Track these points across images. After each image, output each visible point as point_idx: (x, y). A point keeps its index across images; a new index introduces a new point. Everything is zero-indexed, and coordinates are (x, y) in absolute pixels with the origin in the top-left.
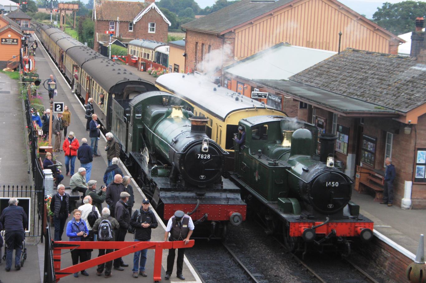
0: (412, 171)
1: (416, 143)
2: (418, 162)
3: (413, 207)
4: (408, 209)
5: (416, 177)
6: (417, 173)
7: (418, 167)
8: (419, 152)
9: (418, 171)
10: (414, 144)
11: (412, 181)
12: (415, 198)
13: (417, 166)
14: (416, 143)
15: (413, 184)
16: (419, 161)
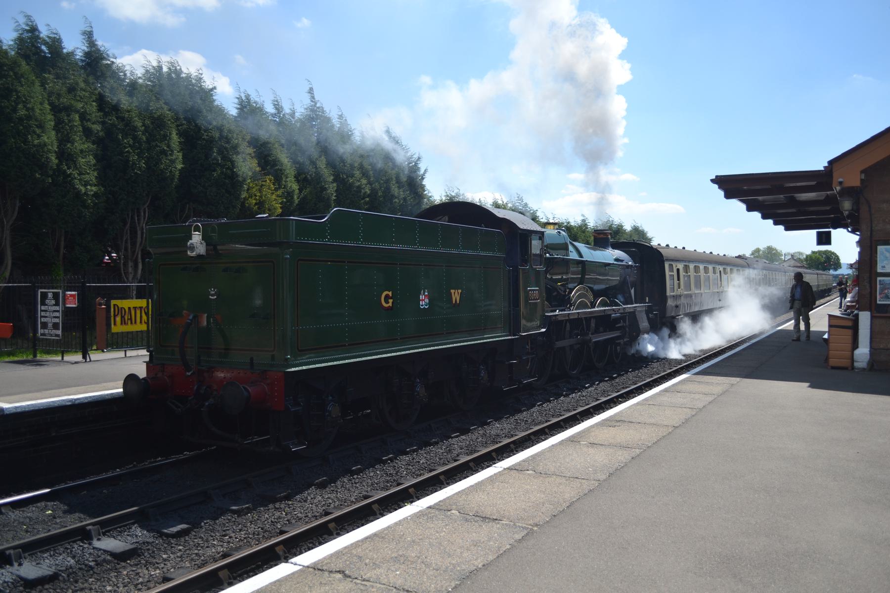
0: (869, 290)
1: (872, 231)
2: (879, 270)
3: (874, 364)
4: (864, 369)
5: (878, 302)
6: (880, 294)
7: (880, 281)
8: (881, 248)
9: (882, 290)
10: (869, 234)
11: (870, 310)
12: (881, 347)
13: (879, 279)
14: (872, 231)
15: (872, 317)
16: (884, 267)
